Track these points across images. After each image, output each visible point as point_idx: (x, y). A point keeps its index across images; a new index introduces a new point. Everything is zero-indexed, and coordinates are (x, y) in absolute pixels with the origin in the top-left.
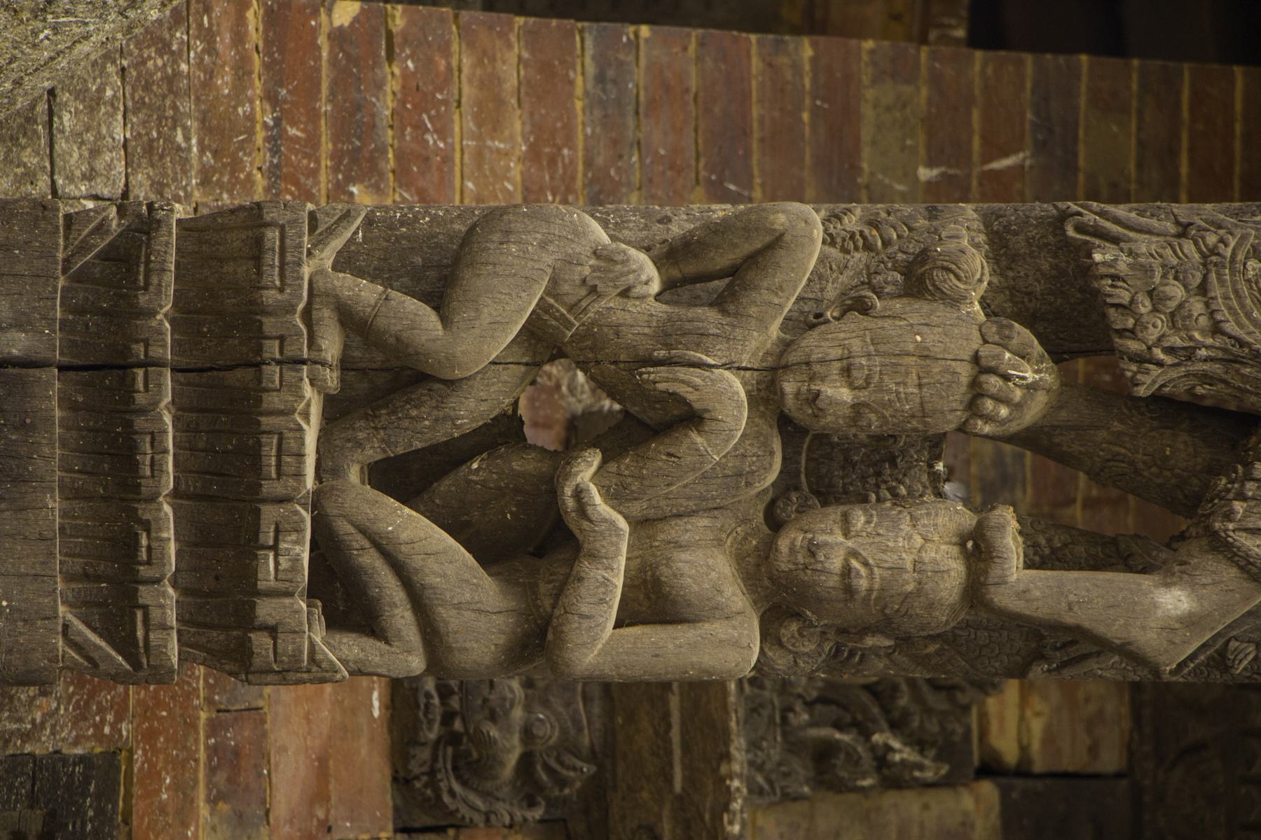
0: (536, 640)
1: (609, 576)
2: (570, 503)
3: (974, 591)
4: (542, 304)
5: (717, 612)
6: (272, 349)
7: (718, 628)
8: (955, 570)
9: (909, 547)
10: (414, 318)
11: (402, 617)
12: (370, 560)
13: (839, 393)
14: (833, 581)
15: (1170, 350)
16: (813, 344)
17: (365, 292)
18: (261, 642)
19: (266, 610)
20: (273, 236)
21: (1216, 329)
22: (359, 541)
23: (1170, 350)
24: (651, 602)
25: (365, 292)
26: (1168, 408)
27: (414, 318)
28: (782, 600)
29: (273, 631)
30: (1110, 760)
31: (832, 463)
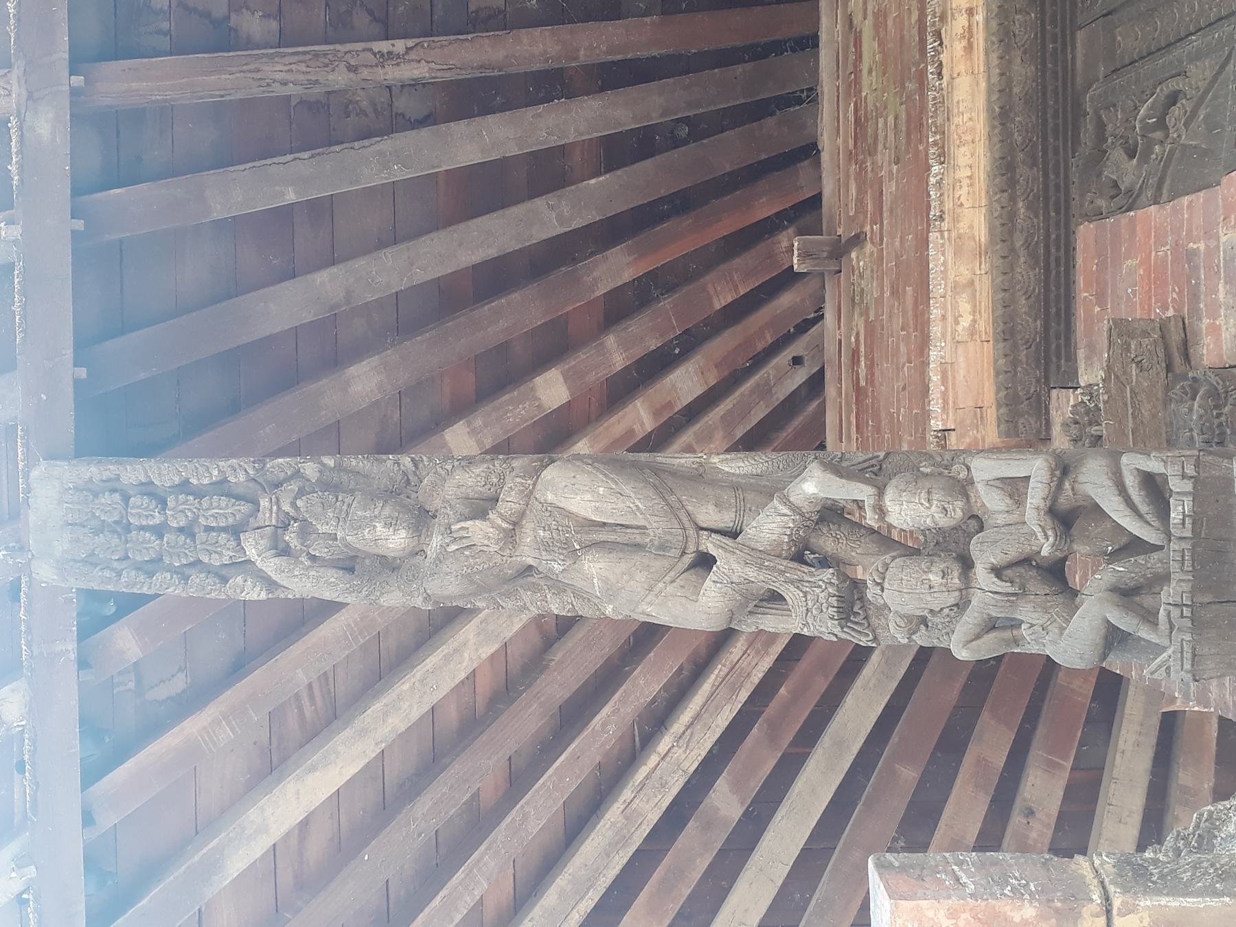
0: (1064, 469)
1: (1036, 496)
2: (1050, 533)
3: (881, 493)
4: (1068, 621)
5: (987, 483)
6: (1187, 612)
7: (987, 476)
8: (889, 501)
9: (908, 510)
10: (1124, 621)
11: (1131, 481)
12: (1144, 508)
13: (935, 578)
14: (935, 497)
15: (820, 587)
16: (952, 598)
17: (1144, 633)
18: (1190, 471)
19: (1188, 486)
20: (1187, 666)
21: (805, 594)
22: (1148, 517)
23: (820, 587)
24: (1015, 488)
25: (1144, 633)
26: (824, 563)
27: (1124, 621)
28: (963, 488)
29: (1184, 476)
30: (1054, 393)
31: (953, 546)
